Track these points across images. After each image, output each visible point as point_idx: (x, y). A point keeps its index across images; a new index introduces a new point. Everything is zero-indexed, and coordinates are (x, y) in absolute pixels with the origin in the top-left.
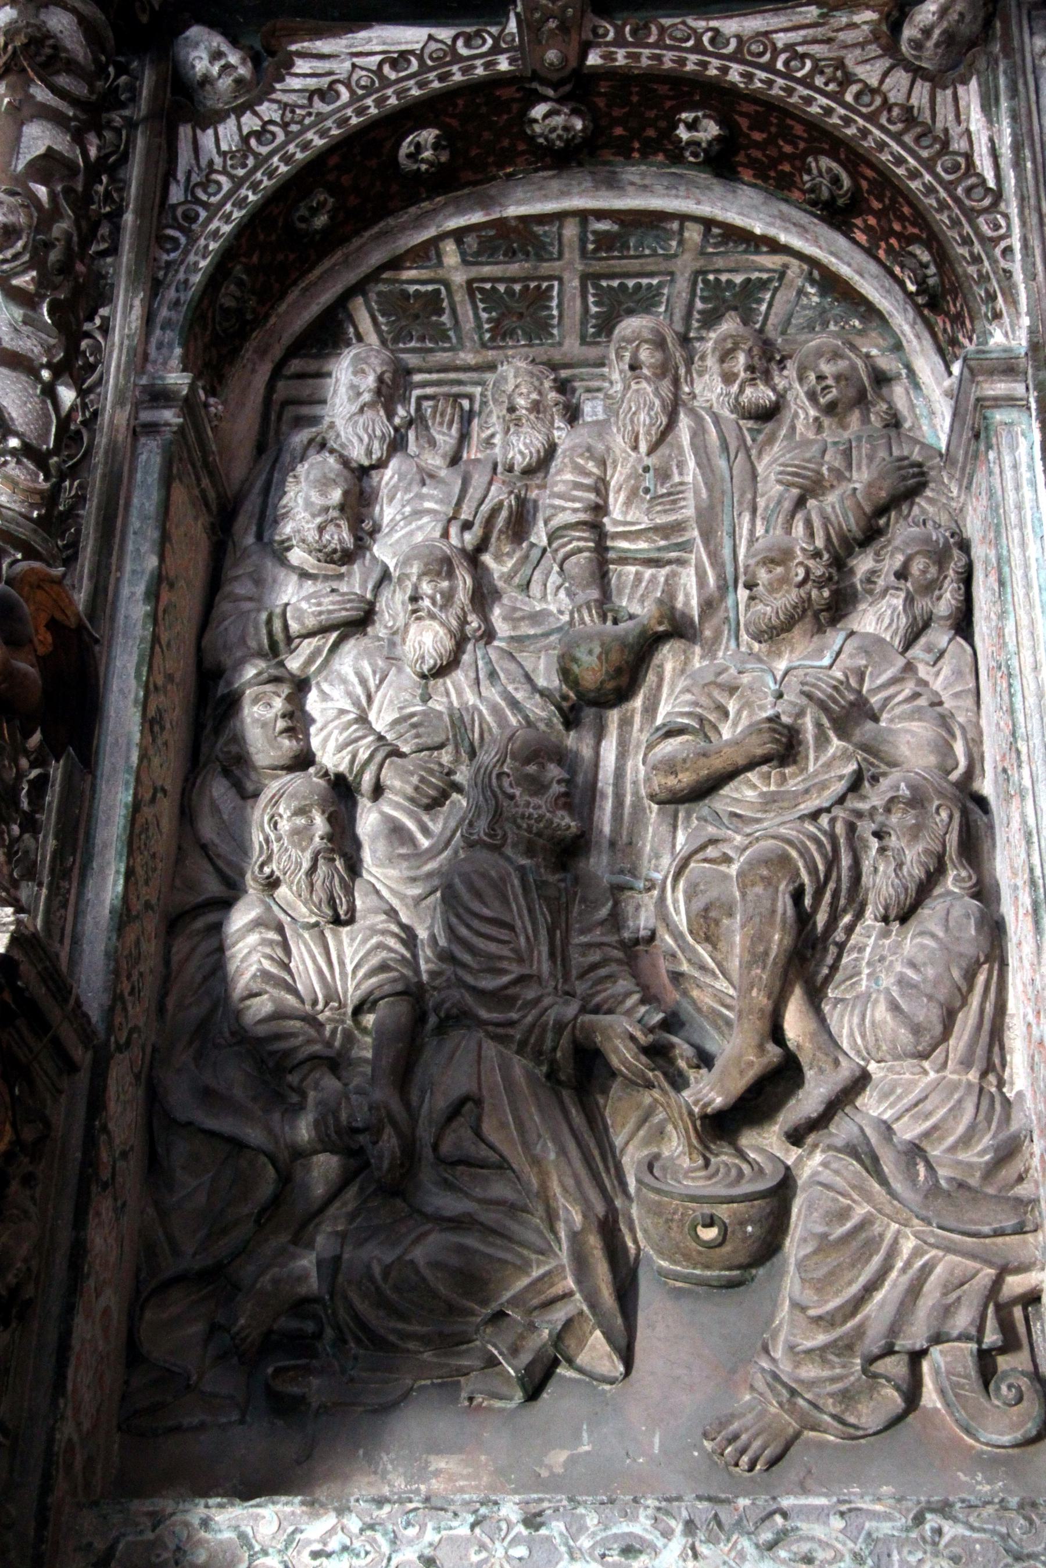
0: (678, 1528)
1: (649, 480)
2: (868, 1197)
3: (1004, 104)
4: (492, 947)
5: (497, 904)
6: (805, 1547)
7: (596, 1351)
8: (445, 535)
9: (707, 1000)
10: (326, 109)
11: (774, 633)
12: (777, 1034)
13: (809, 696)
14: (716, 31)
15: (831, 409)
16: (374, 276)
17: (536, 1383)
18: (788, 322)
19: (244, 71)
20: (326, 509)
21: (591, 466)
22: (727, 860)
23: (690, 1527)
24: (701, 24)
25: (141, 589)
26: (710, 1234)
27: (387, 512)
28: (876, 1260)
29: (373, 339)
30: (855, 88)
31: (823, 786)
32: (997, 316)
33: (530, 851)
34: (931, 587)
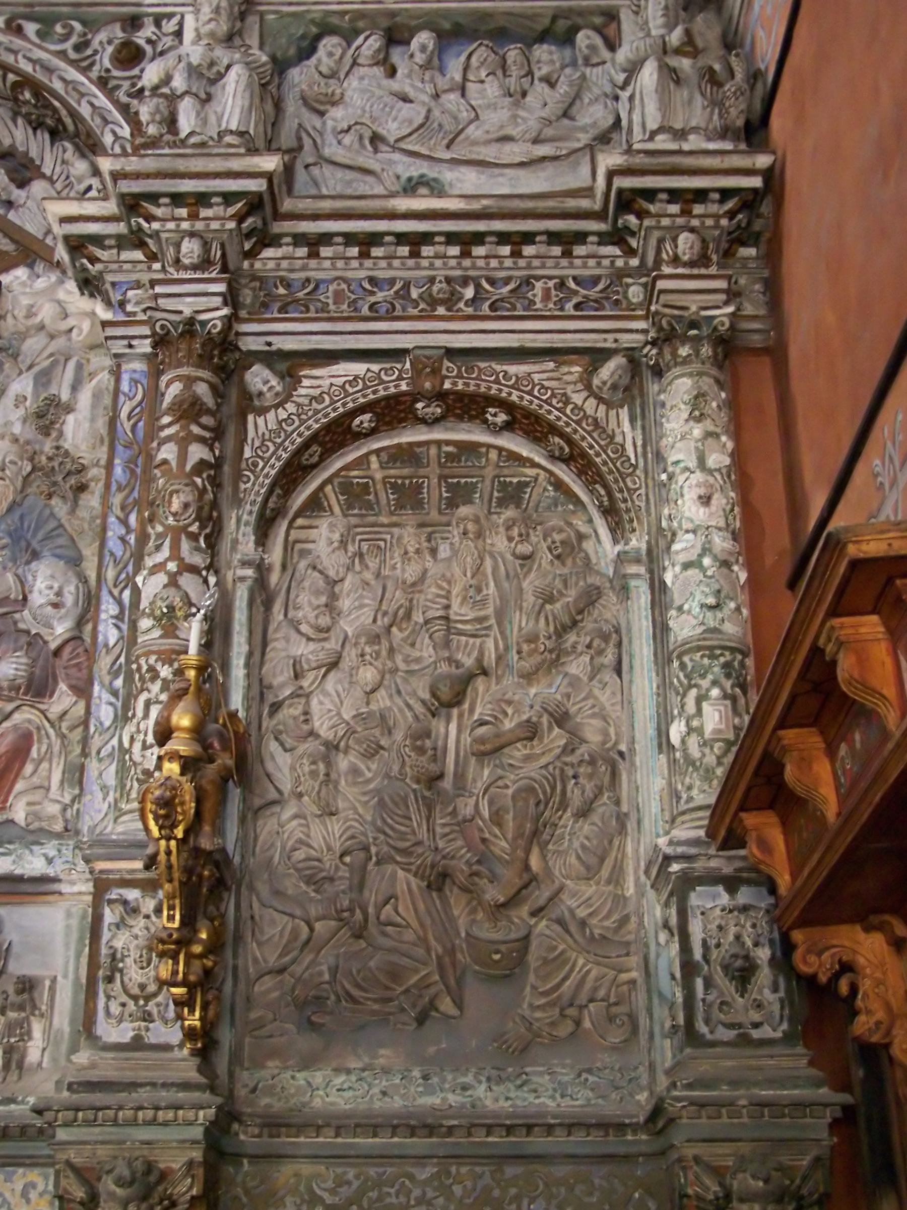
0: (483, 1079)
1: (472, 592)
2: (564, 941)
3: (639, 423)
4: (403, 828)
5: (403, 807)
6: (533, 1087)
7: (446, 1005)
8: (375, 621)
9: (497, 851)
10: (320, 407)
11: (528, 677)
12: (527, 867)
13: (546, 710)
14: (506, 372)
15: (558, 557)
16: (336, 474)
17: (422, 1019)
18: (537, 506)
19: (279, 388)
20: (318, 607)
21: (445, 585)
22: (507, 787)
23: (489, 1079)
24: (498, 368)
25: (242, 662)
26: (497, 957)
27: (345, 604)
28: (567, 968)
29: (337, 509)
30: (570, 407)
31: (550, 750)
32: (634, 530)
33: (418, 782)
34: (600, 652)
